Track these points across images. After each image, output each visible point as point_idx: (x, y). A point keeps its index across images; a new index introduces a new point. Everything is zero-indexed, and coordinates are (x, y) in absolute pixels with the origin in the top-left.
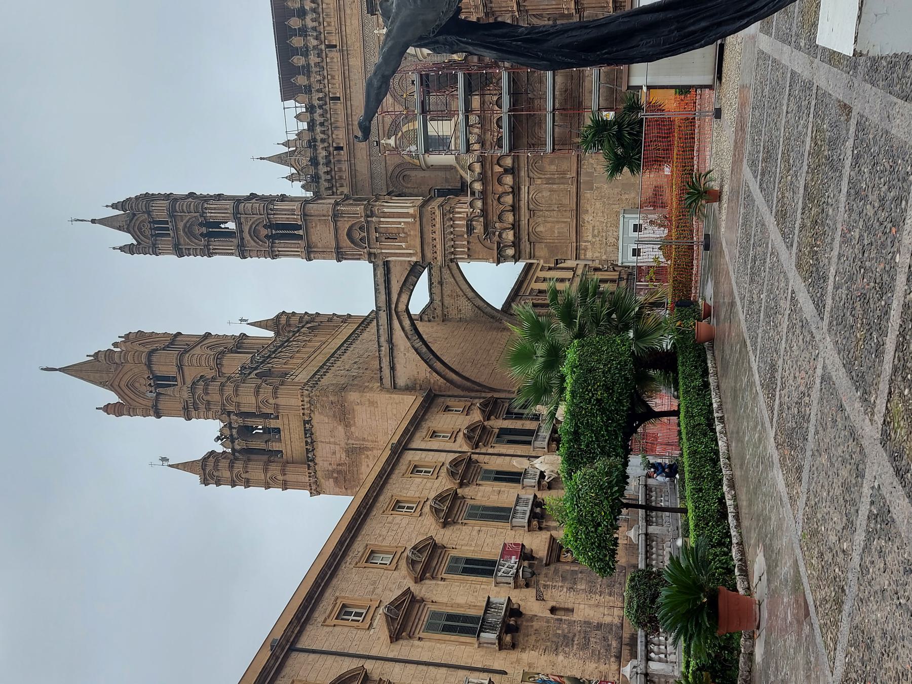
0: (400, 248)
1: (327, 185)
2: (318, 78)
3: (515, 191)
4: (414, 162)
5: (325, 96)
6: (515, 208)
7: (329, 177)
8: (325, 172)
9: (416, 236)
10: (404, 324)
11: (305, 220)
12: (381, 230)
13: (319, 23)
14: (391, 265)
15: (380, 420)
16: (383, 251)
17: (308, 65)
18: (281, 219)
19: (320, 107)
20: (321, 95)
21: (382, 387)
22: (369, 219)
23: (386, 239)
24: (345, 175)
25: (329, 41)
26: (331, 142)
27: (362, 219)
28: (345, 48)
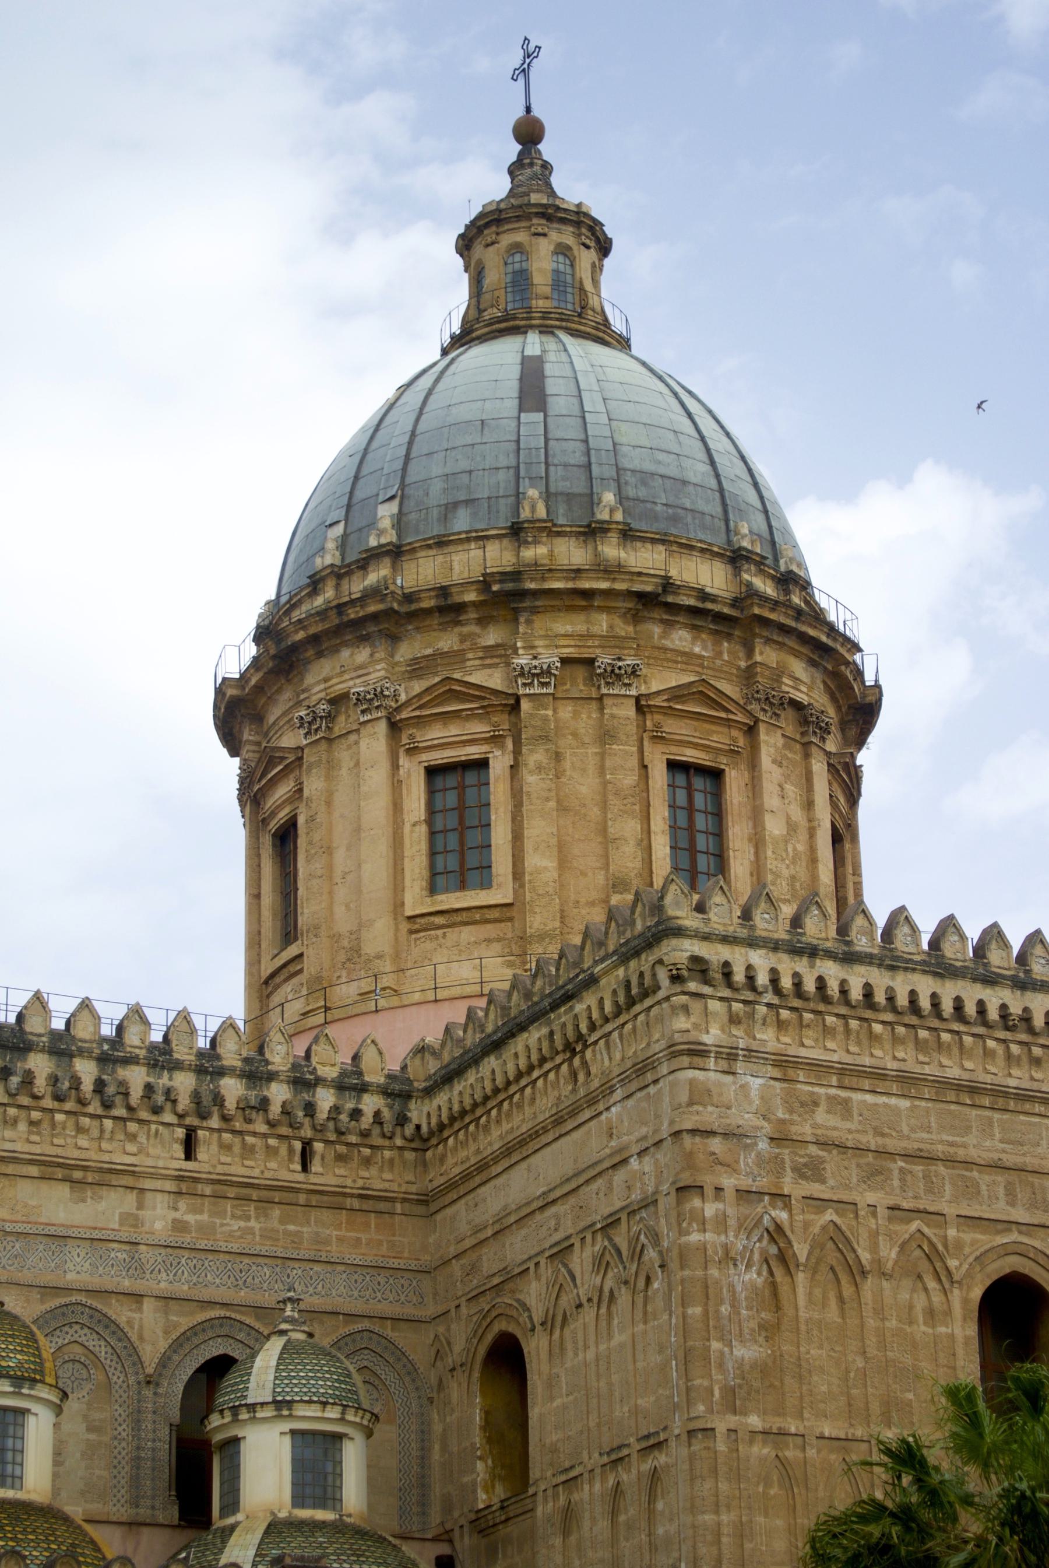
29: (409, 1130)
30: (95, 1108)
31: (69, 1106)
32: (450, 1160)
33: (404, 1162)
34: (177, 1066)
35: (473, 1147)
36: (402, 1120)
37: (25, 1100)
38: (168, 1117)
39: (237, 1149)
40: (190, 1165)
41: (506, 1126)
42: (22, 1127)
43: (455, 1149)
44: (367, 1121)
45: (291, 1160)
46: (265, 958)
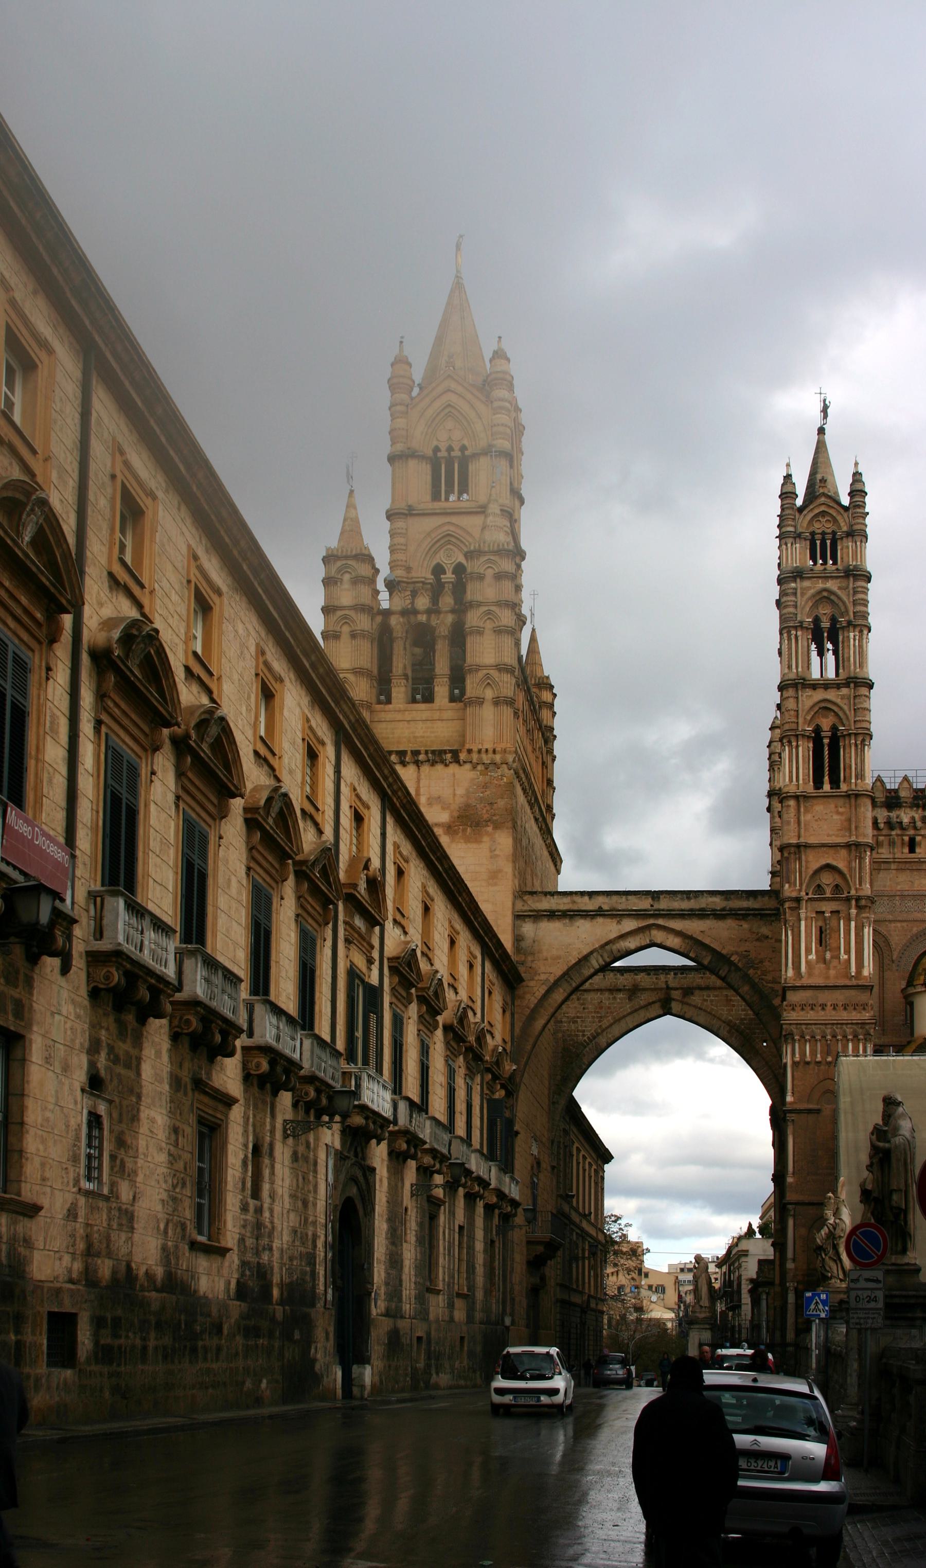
0: (809, 951)
4: (920, 974)
9: (827, 978)
10: (630, 939)
22: (853, 902)
23: (821, 928)
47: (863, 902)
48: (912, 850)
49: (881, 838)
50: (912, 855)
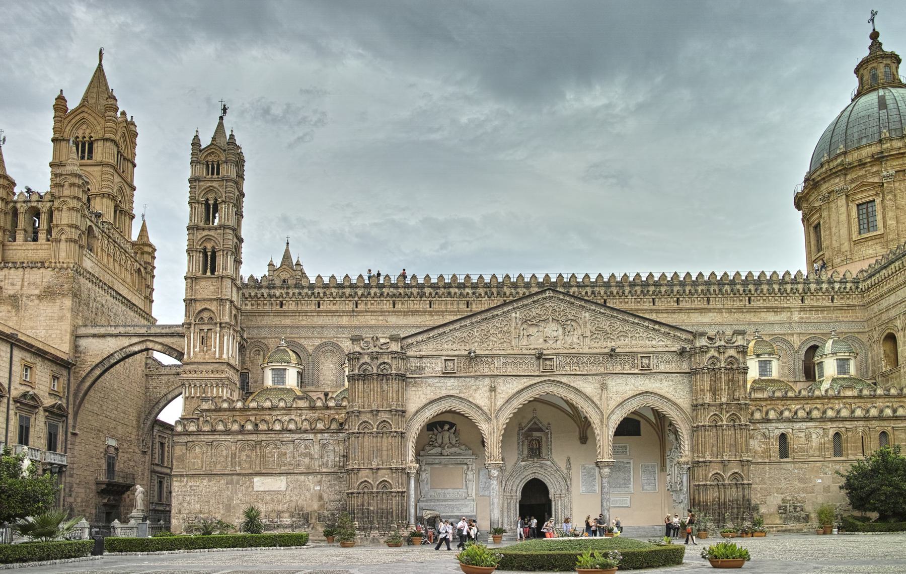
0: (195, 347)
1: (253, 294)
2: (335, 294)
3: (227, 432)
5: (321, 298)
6: (213, 432)
7: (259, 296)
8: (263, 293)
11: (218, 277)
12: (209, 334)
13: (374, 297)
14: (182, 339)
15: (45, 324)
16: (192, 334)
17: (344, 288)
18: (220, 260)
19: (313, 294)
20: (322, 295)
21: (75, 327)
22: (218, 325)
24: (261, 308)
25: (360, 304)
26: (287, 299)
27: (218, 320)
28: (355, 314)
29: (859, 290)
30: (779, 295)
31: (772, 295)
32: (871, 295)
33: (858, 298)
34: (799, 283)
35: (878, 292)
36: (857, 288)
37: (762, 295)
38: (797, 295)
39: (815, 300)
40: (803, 304)
41: (888, 286)
42: (761, 301)
43: (872, 293)
44: (848, 290)
45: (829, 300)
46: (813, 256)
47: (224, 325)
48: (281, 307)
49: (265, 302)
50: (281, 309)
